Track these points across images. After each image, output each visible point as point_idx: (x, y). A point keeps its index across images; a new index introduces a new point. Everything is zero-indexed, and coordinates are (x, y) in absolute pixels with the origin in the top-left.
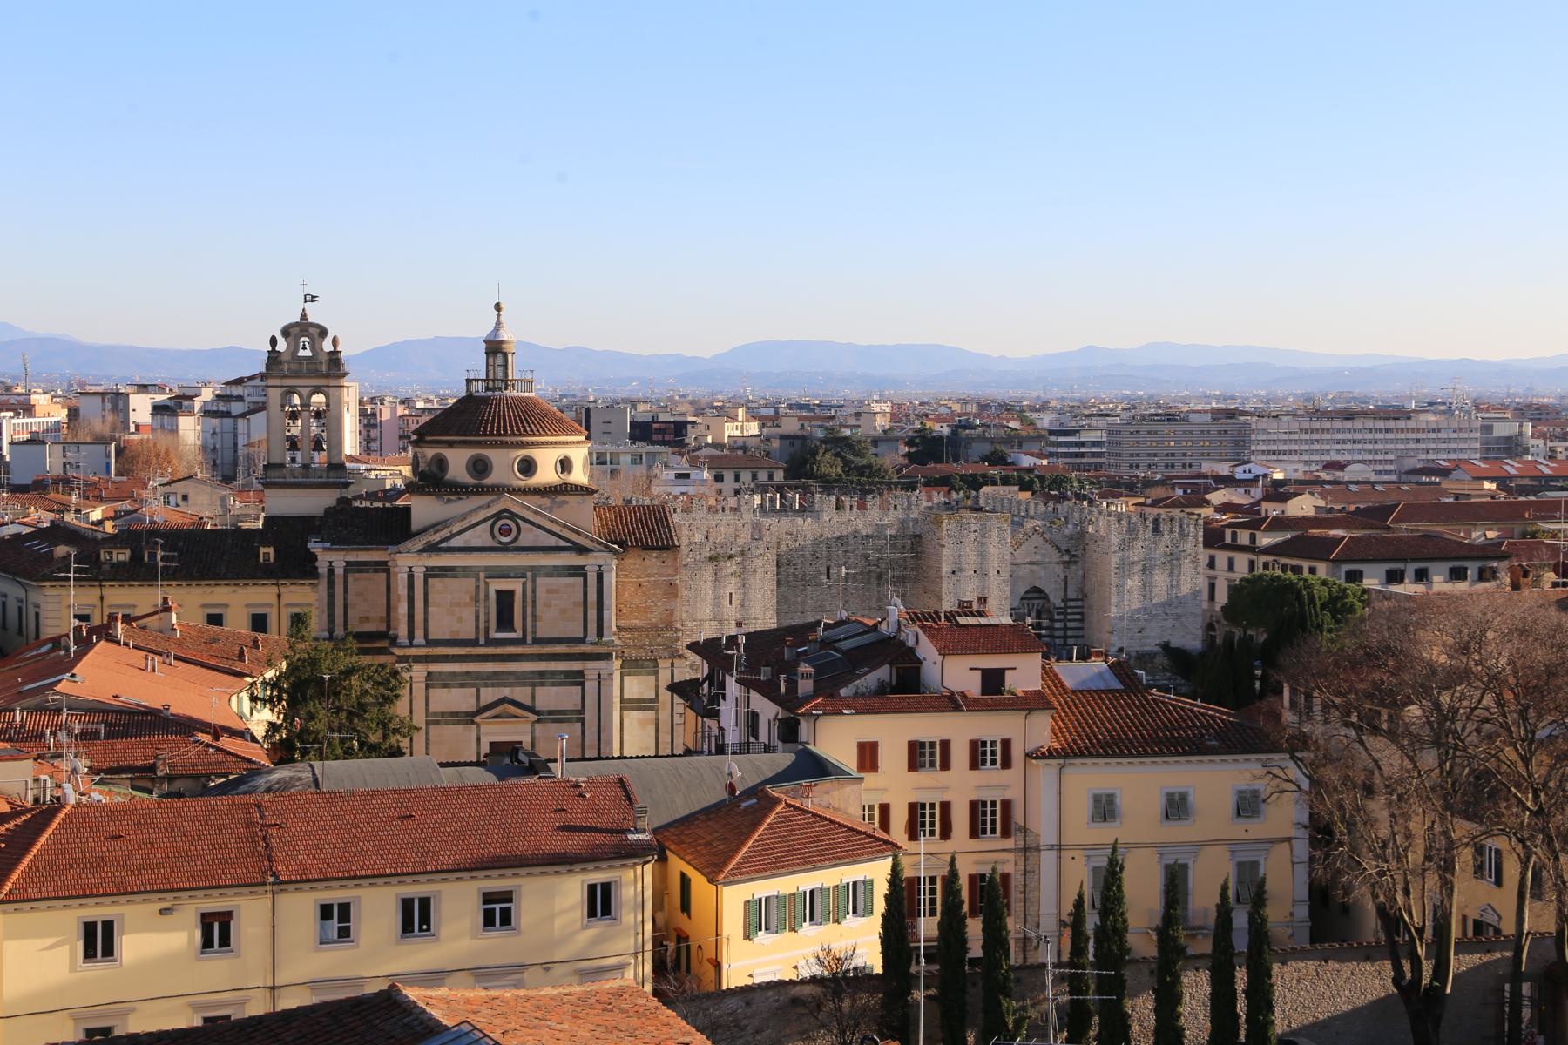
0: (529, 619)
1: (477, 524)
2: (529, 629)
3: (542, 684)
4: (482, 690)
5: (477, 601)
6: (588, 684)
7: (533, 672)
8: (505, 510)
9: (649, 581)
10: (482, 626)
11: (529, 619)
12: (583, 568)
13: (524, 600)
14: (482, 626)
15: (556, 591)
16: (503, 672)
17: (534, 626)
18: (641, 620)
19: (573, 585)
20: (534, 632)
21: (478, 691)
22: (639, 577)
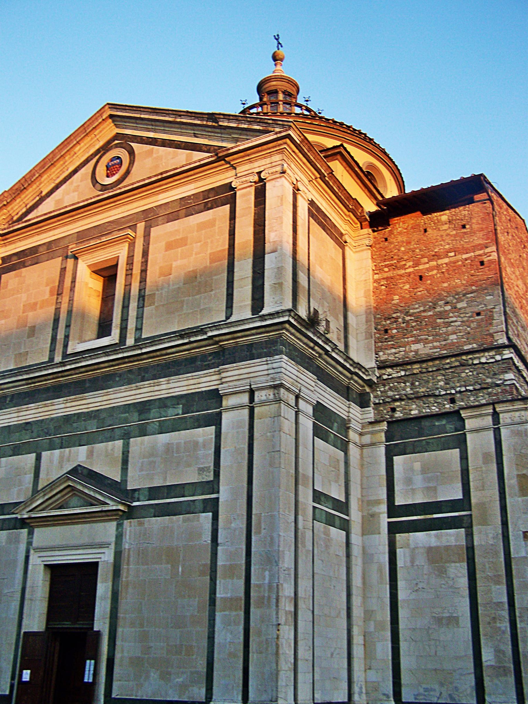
0: (133, 305)
1: (75, 171)
2: (132, 324)
3: (143, 432)
4: (45, 454)
5: (59, 294)
6: (226, 418)
7: (127, 408)
8: (117, 136)
9: (438, 267)
10: (60, 336)
11: (133, 305)
12: (229, 187)
13: (129, 274)
14: (60, 336)
15: (183, 242)
16: (79, 415)
17: (140, 317)
18: (426, 342)
19: (211, 223)
20: (139, 329)
21: (38, 458)
22: (416, 264)
